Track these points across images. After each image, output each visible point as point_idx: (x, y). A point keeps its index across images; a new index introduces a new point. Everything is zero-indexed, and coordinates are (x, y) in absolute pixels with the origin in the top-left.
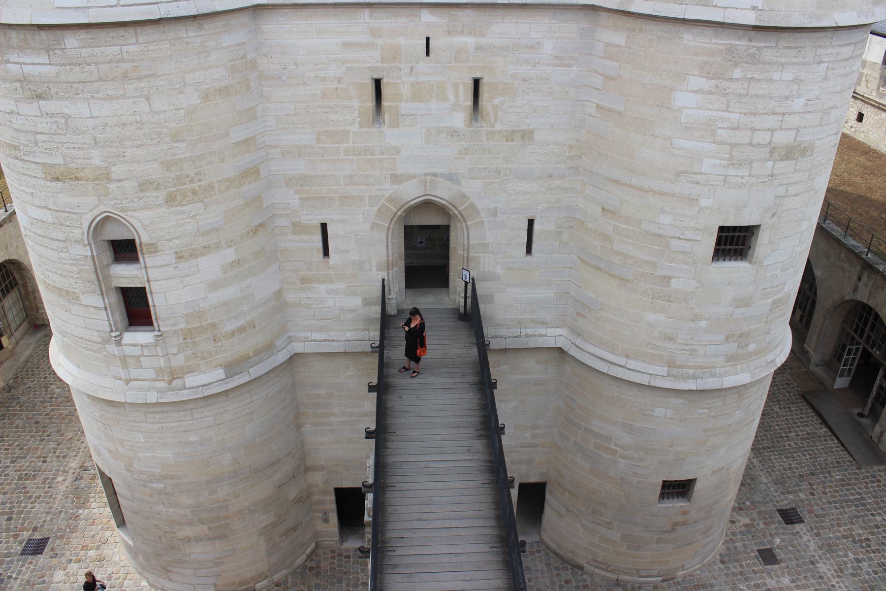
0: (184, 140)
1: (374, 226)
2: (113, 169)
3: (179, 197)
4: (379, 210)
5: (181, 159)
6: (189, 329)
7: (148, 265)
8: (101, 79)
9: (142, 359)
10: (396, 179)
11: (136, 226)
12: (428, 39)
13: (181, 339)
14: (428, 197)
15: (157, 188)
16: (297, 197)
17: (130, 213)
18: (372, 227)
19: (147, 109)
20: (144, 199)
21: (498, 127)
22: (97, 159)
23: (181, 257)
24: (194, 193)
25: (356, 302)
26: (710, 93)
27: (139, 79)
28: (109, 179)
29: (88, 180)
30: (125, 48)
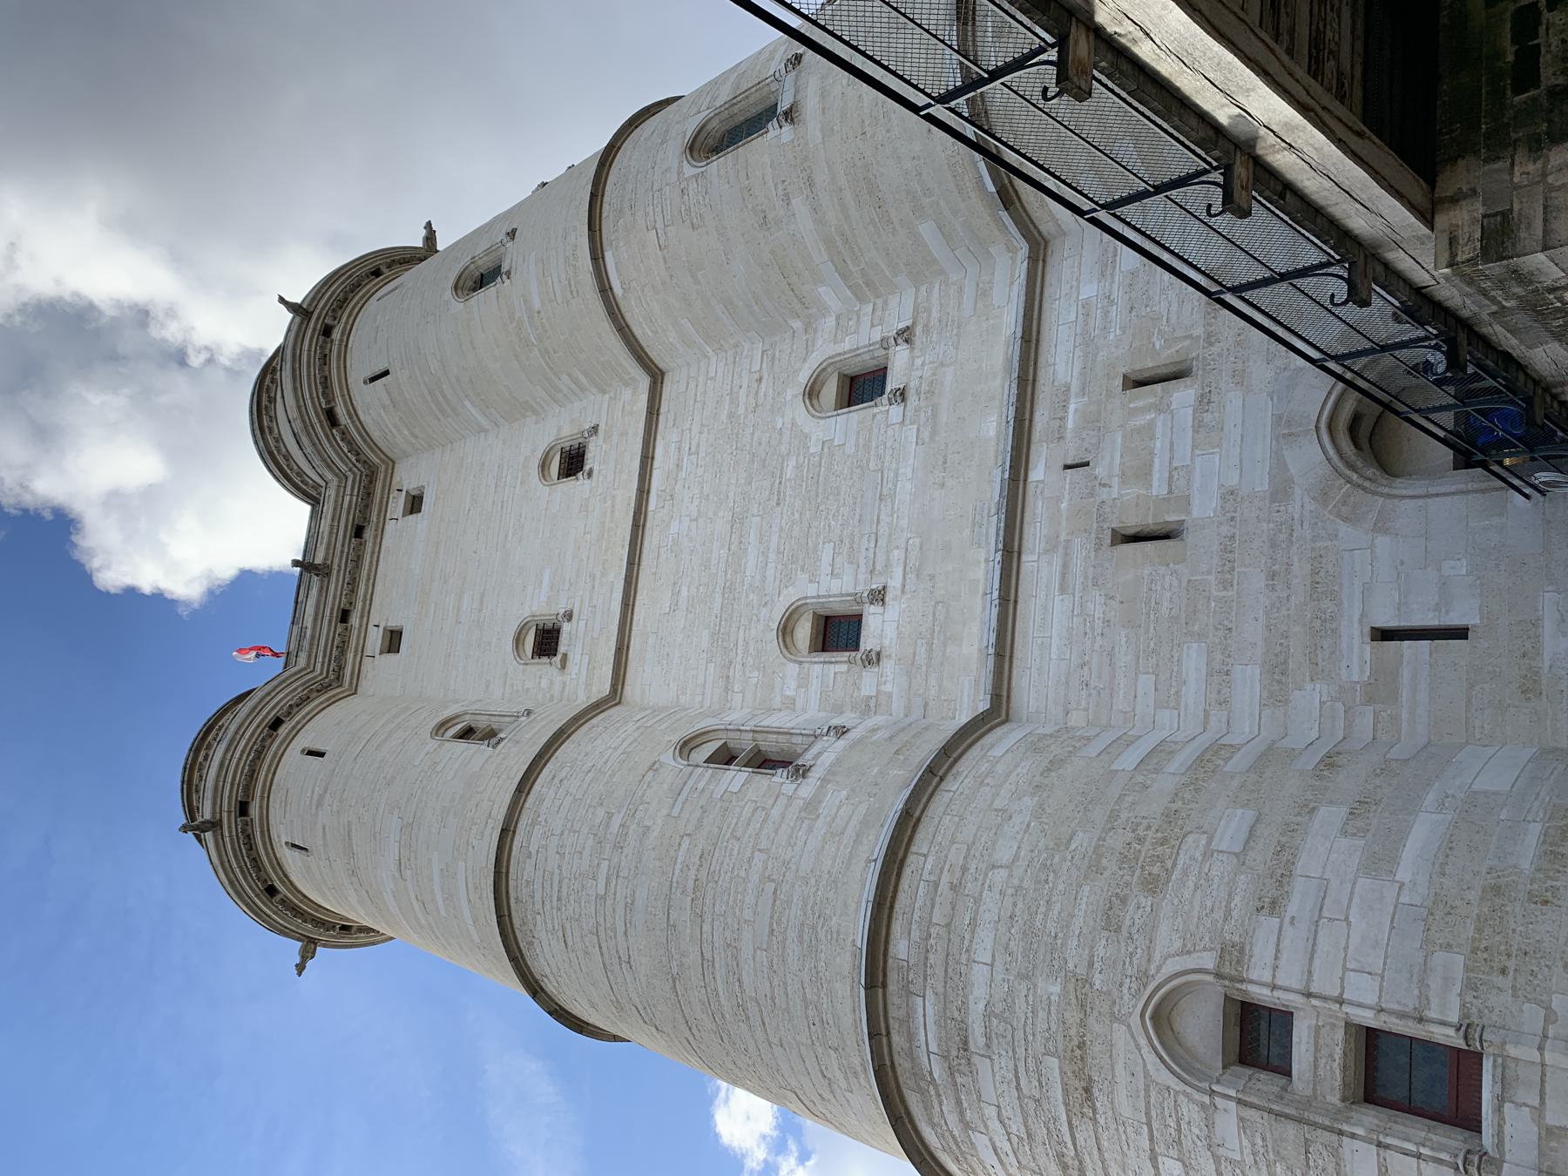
0: (1074, 834)
1: (1381, 527)
2: (1071, 965)
3: (1155, 870)
4: (1346, 519)
5: (1097, 847)
6: (1474, 951)
7: (1267, 976)
9: (1551, 1119)
10: (1281, 491)
11: (1179, 968)
12: (1067, 467)
13: (1499, 980)
14: (1323, 426)
15: (1124, 901)
16: (1309, 687)
17: (1153, 968)
18: (1386, 532)
19: (1003, 873)
20: (1134, 930)
24: (1164, 842)
27: (964, 869)
28: (1088, 981)
29: (1083, 1024)
30: (926, 876)
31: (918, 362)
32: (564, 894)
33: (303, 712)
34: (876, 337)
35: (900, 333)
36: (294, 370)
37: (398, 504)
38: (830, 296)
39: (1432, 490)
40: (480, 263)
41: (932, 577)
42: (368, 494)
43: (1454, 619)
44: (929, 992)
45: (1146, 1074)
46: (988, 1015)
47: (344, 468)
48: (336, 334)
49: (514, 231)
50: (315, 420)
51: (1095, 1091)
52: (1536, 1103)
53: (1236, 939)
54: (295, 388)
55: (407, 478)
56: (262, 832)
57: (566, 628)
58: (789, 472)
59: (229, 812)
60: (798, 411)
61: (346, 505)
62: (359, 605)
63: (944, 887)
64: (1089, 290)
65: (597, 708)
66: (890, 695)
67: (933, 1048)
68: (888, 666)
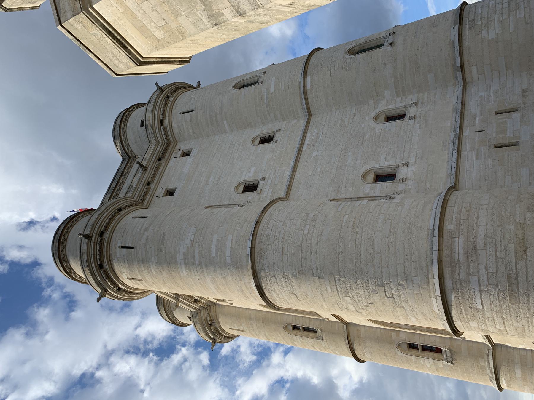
21: (520, 101)
26: (488, 28)
32: (286, 236)
35: (414, 103)
38: (387, 94)
39: (457, 244)
40: (245, 81)
42: (166, 150)
44: (461, 237)
47: (160, 139)
48: (171, 99)
50: (156, 122)
51: (528, 251)
56: (107, 243)
57: (261, 183)
59: (96, 234)
61: (157, 151)
62: (155, 182)
64: (482, 94)
65: (281, 199)
66: (410, 189)
67: (461, 251)
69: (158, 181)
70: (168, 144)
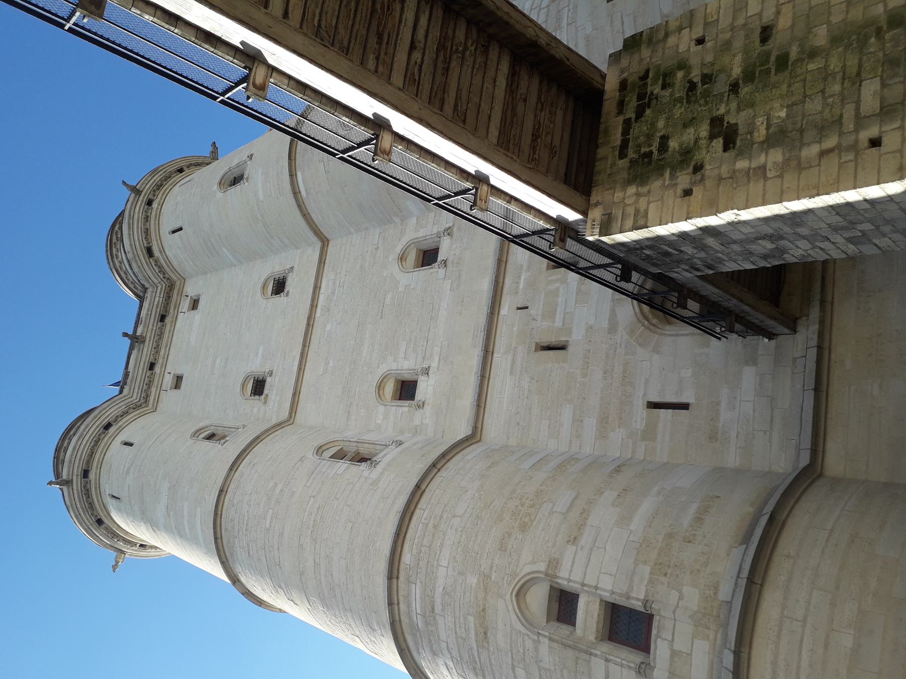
1: (656, 350)
3: (526, 520)
4: (640, 345)
7: (566, 576)
8: (430, 546)
10: (613, 328)
11: (529, 570)
12: (519, 308)
15: (510, 535)
16: (617, 430)
18: (658, 352)
19: (459, 519)
22: (473, 580)
23: (575, 539)
25: (749, 375)
27: (441, 517)
28: (488, 577)
29: (485, 599)
31: (454, 246)
33: (124, 420)
34: (435, 231)
36: (129, 224)
37: (186, 304)
41: (452, 363)
43: (683, 400)
44: (418, 581)
45: (511, 625)
46: (445, 592)
47: (156, 281)
49: (252, 155)
50: (140, 253)
51: (489, 634)
52: (670, 639)
53: (556, 556)
54: (129, 235)
55: (191, 289)
56: (96, 488)
57: (269, 380)
58: (388, 301)
60: (395, 268)
62: (160, 361)
63: (430, 526)
65: (279, 425)
67: (419, 611)
68: (428, 409)
69: (163, 358)
70: (171, 286)
